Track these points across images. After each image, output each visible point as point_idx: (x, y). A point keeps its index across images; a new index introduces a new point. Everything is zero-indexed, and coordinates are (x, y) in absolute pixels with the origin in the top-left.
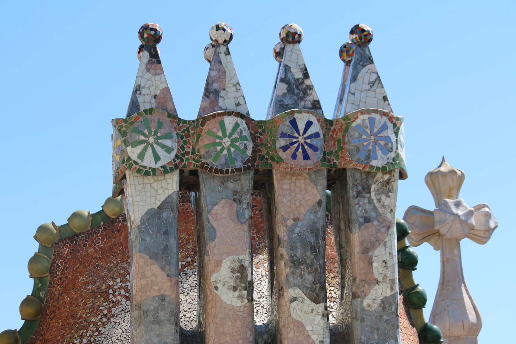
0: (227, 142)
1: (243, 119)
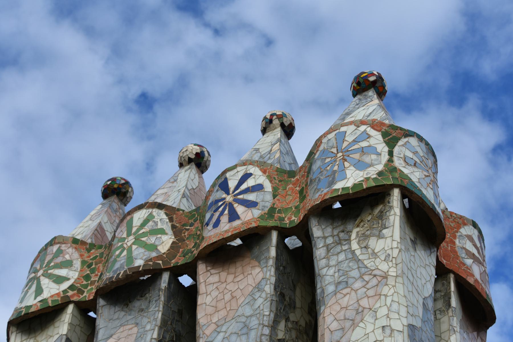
1: (161, 209)
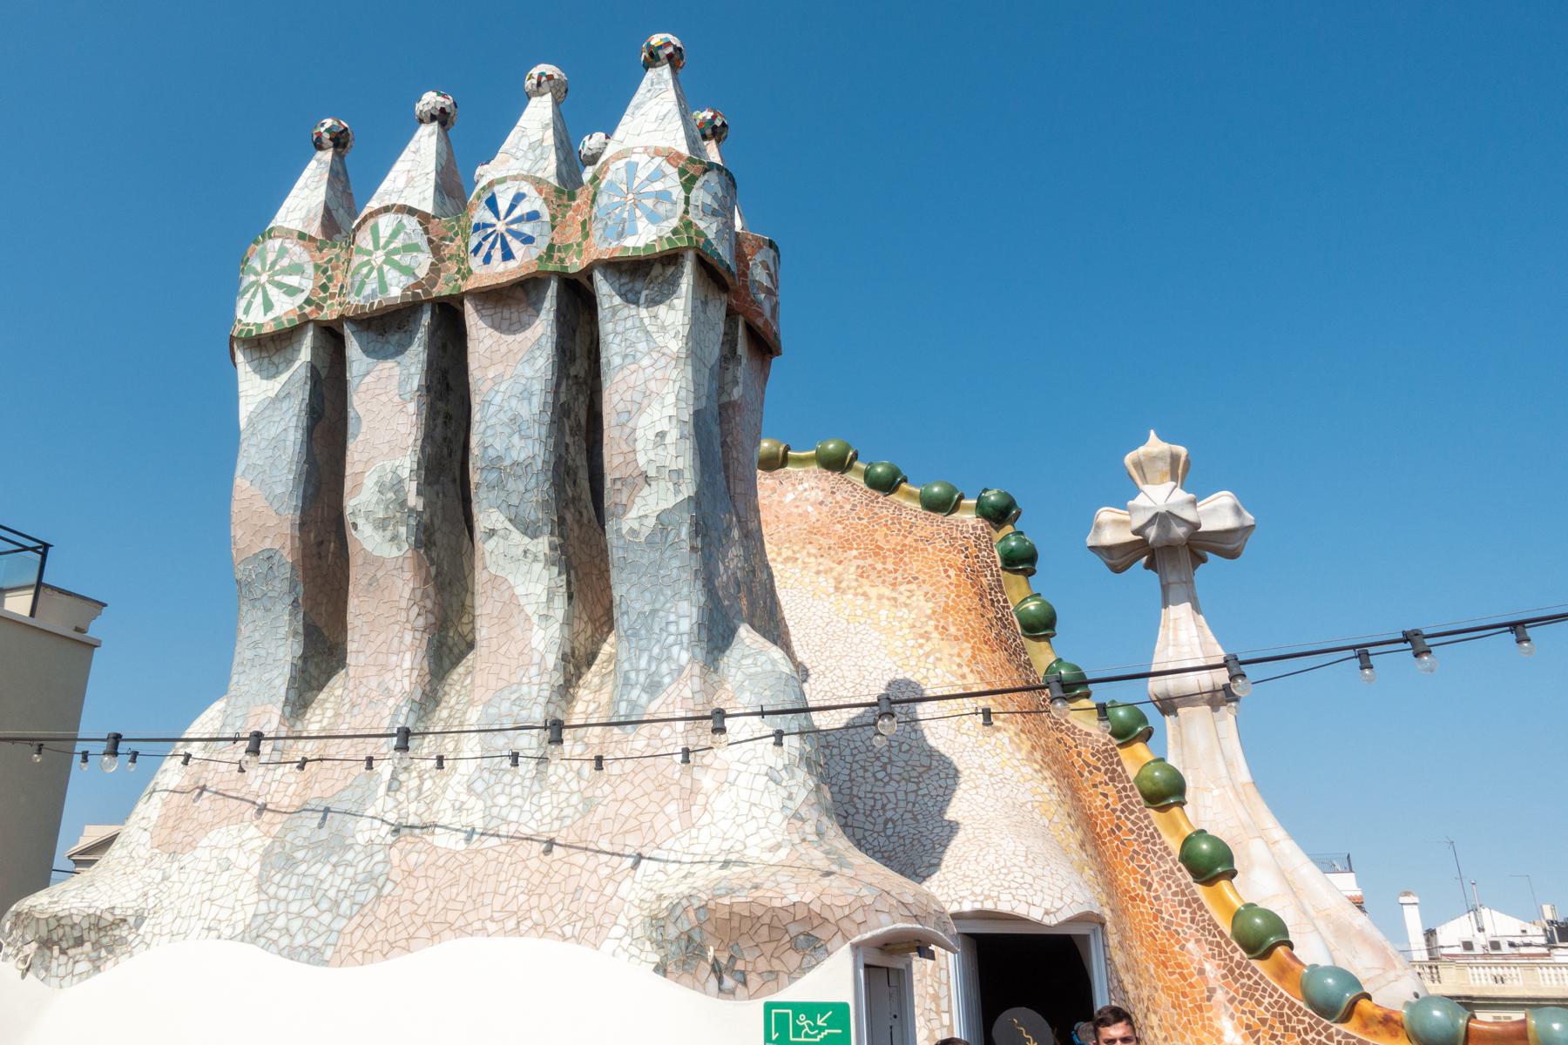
0: (379, 257)
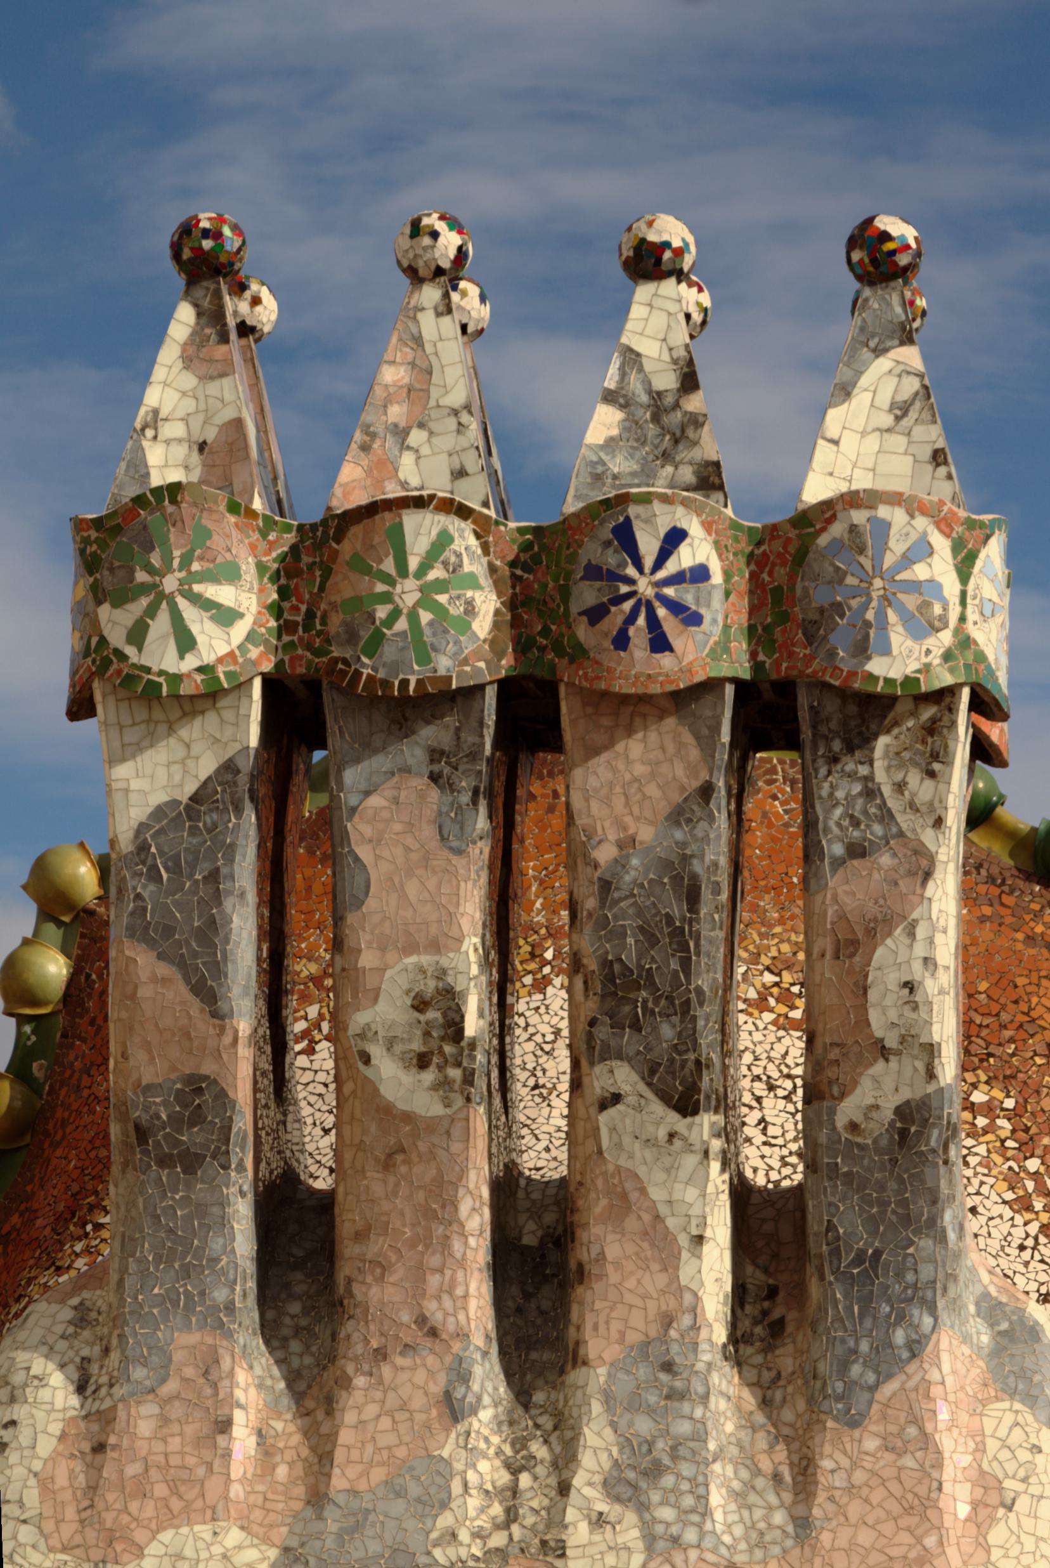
1: (465, 519)
